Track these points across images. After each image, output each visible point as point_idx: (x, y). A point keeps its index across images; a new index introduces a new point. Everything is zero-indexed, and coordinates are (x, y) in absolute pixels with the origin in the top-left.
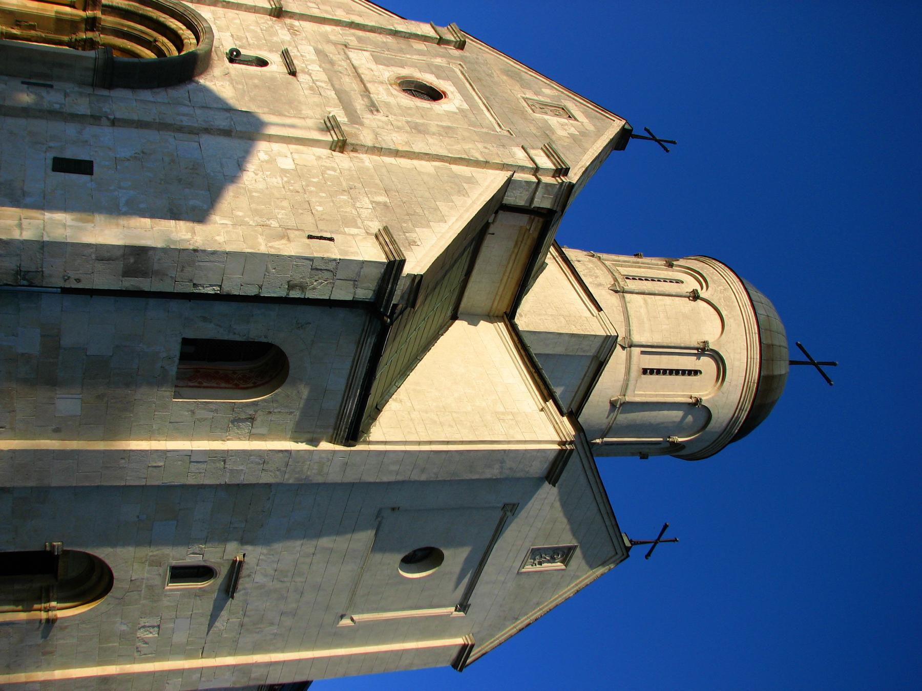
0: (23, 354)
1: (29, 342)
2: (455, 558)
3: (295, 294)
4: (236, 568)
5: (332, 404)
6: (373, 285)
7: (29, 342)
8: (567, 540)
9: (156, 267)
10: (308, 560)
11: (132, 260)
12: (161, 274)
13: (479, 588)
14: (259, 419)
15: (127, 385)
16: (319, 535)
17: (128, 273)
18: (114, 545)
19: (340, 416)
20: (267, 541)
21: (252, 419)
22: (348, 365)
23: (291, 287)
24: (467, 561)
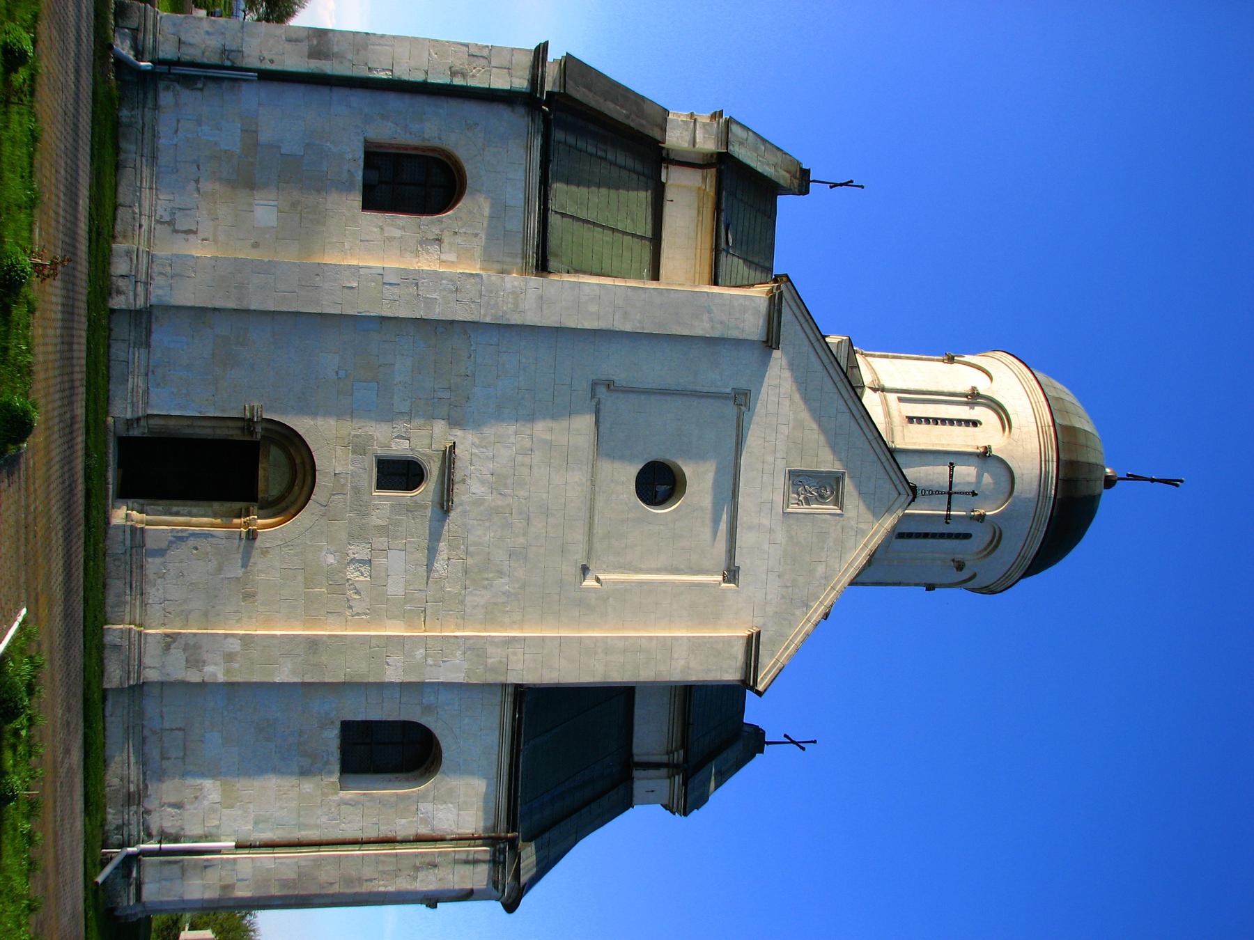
0: (226, 152)
2: (700, 479)
3: (458, 81)
5: (515, 224)
6: (527, 74)
7: (230, 138)
8: (827, 462)
9: (336, 49)
10: (527, 460)
11: (315, 42)
12: (340, 56)
14: (446, 240)
15: (319, 191)
16: (532, 418)
18: (314, 414)
20: (477, 425)
21: (439, 240)
22: (520, 174)
23: (453, 74)
24: (717, 484)
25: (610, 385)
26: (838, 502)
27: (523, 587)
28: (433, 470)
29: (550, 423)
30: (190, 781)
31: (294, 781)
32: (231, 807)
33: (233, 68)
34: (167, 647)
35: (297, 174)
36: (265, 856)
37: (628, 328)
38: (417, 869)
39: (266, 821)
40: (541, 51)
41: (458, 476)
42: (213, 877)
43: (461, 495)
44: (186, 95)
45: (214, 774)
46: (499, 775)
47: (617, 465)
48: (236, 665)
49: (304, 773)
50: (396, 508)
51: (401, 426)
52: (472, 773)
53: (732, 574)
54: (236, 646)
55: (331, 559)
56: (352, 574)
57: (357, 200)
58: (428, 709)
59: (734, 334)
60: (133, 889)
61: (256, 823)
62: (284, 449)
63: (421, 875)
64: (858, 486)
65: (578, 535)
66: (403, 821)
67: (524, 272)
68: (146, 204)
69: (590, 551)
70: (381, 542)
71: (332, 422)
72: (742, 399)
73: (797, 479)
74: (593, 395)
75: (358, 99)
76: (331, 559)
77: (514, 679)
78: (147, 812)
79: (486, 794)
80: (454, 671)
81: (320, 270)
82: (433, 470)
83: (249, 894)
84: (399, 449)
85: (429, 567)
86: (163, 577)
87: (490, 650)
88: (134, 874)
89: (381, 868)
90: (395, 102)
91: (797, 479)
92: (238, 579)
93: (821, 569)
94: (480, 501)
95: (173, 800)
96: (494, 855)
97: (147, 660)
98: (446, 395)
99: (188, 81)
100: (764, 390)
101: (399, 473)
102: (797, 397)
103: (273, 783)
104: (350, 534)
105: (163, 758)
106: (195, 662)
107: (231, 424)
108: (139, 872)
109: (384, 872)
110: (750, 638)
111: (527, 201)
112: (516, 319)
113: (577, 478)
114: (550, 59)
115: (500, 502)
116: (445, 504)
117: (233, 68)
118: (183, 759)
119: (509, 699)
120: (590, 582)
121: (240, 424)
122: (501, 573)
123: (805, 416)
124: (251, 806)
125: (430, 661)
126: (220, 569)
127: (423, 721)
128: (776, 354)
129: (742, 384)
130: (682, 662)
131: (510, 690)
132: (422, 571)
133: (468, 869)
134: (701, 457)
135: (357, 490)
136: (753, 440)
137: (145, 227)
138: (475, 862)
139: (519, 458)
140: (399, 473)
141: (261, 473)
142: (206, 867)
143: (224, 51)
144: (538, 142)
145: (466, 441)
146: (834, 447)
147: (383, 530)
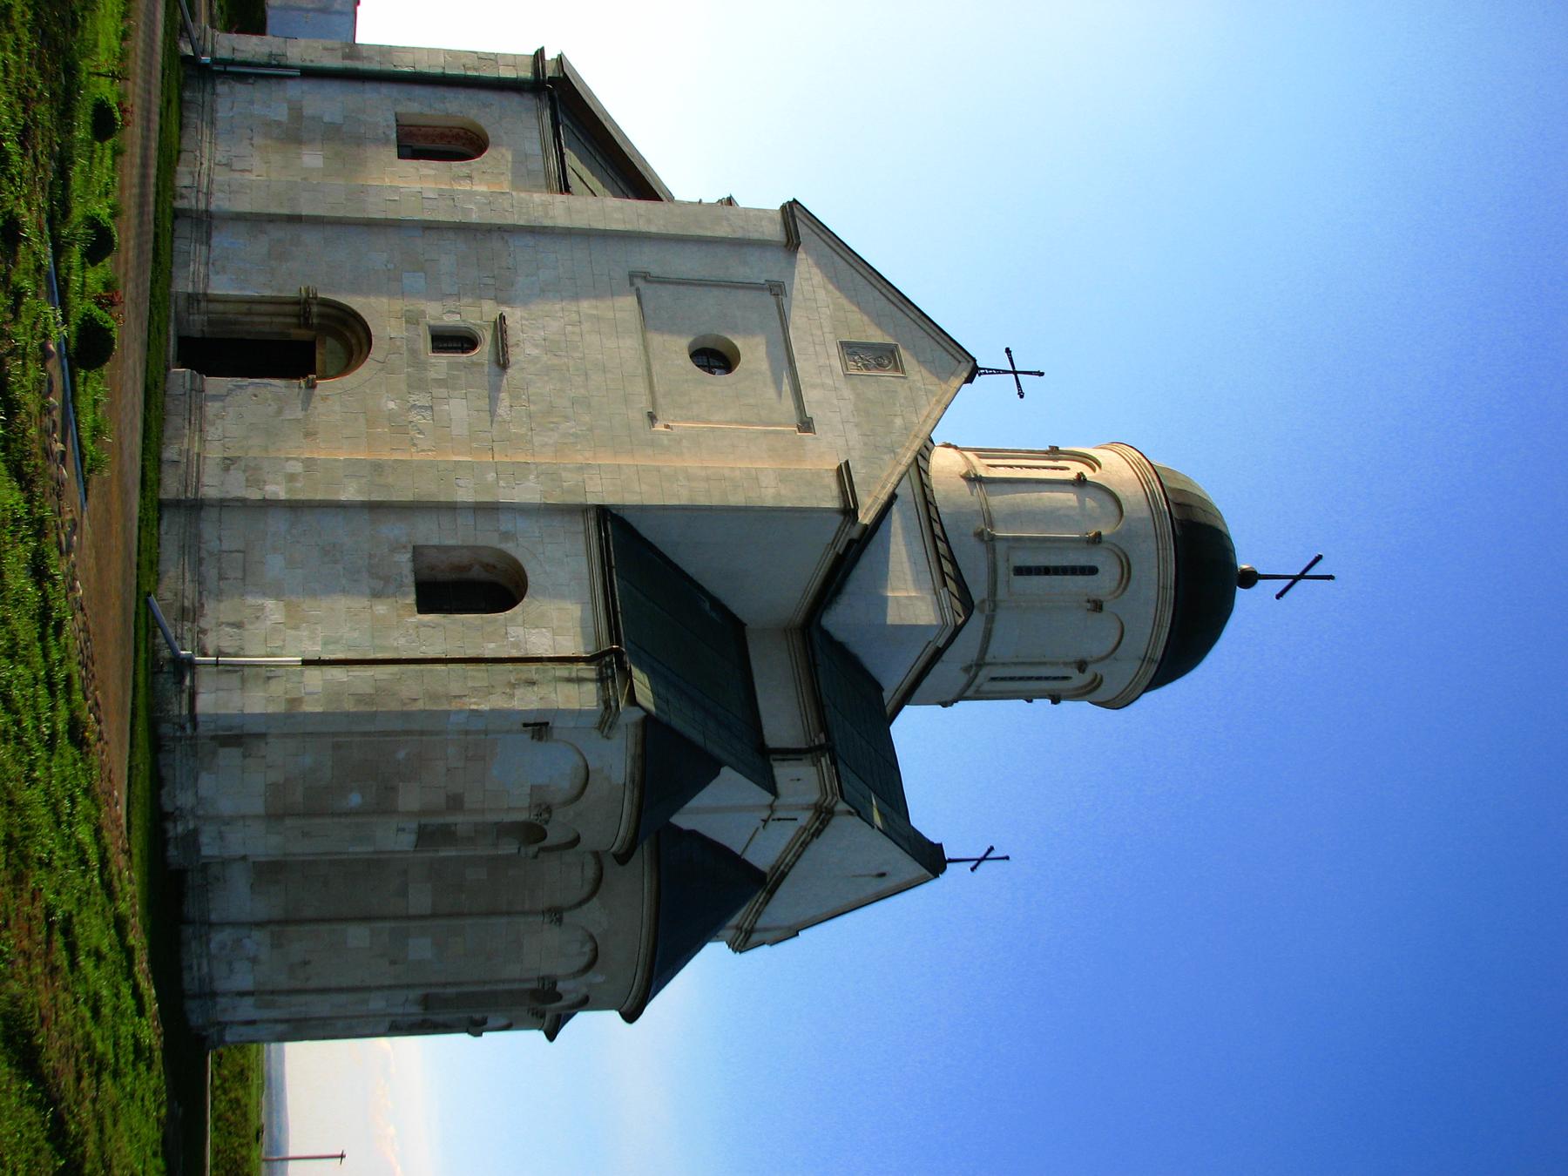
1: (281, 113)
2: (753, 352)
4: (500, 325)
5: (537, 164)
7: (281, 113)
8: (877, 336)
10: (577, 329)
13: (809, 396)
14: (474, 174)
15: (358, 145)
16: (576, 297)
17: (345, 57)
19: (547, 175)
20: (525, 304)
21: (470, 177)
22: (536, 134)
25: (646, 277)
26: (898, 366)
27: (591, 429)
28: (487, 337)
29: (594, 302)
30: (250, 600)
31: (365, 602)
32: (296, 628)
33: (278, 66)
34: (227, 469)
35: (344, 138)
36: (338, 673)
37: (653, 229)
38: (513, 686)
39: (336, 642)
40: (540, 54)
41: (511, 340)
42: (277, 688)
43: (514, 355)
44: (239, 88)
45: (277, 592)
46: (592, 590)
47: (666, 337)
48: (299, 485)
49: (376, 595)
50: (451, 366)
51: (451, 304)
52: (562, 597)
53: (806, 425)
54: (298, 468)
55: (392, 405)
56: (414, 417)
57: (394, 151)
58: (506, 536)
59: (755, 236)
60: (185, 696)
61: (325, 644)
62: (339, 336)
63: (519, 692)
64: (916, 355)
65: (640, 387)
66: (492, 645)
67: (550, 189)
68: (206, 151)
69: (654, 403)
70: (443, 392)
71: (385, 300)
72: (777, 290)
73: (850, 349)
74: (632, 284)
75: (386, 90)
76: (392, 405)
77: (593, 500)
78: (203, 632)
79: (582, 619)
80: (529, 492)
81: (364, 189)
82: (487, 337)
83: (319, 709)
84: (451, 320)
85: (492, 413)
86: (222, 418)
87: (564, 474)
88: (187, 682)
89: (470, 684)
90: (419, 91)
91: (850, 349)
92: (298, 420)
93: (898, 422)
95: (232, 619)
96: (601, 673)
97: (206, 480)
98: (491, 281)
99: (242, 78)
100: (797, 280)
101: (453, 341)
102: (830, 287)
103: (342, 603)
104: (409, 386)
105: (221, 578)
106: (257, 483)
107: (287, 309)
108: (193, 680)
109: (474, 689)
110: (839, 469)
111: (544, 150)
112: (548, 223)
113: (628, 346)
115: (556, 361)
116: (502, 363)
117: (278, 66)
118: (243, 579)
119: (592, 524)
120: (659, 427)
121: (297, 308)
122: (567, 418)
123: (844, 302)
124: (319, 627)
125: (502, 483)
126: (280, 412)
128: (801, 255)
130: (771, 491)
131: (592, 514)
132: (486, 415)
133: (572, 689)
134: (748, 332)
135: (413, 352)
136: (797, 318)
137: (205, 165)
139: (569, 328)
140: (453, 341)
142: (269, 678)
143: (270, 55)
144: (547, 113)
145: (515, 317)
146: (879, 325)
147: (441, 383)
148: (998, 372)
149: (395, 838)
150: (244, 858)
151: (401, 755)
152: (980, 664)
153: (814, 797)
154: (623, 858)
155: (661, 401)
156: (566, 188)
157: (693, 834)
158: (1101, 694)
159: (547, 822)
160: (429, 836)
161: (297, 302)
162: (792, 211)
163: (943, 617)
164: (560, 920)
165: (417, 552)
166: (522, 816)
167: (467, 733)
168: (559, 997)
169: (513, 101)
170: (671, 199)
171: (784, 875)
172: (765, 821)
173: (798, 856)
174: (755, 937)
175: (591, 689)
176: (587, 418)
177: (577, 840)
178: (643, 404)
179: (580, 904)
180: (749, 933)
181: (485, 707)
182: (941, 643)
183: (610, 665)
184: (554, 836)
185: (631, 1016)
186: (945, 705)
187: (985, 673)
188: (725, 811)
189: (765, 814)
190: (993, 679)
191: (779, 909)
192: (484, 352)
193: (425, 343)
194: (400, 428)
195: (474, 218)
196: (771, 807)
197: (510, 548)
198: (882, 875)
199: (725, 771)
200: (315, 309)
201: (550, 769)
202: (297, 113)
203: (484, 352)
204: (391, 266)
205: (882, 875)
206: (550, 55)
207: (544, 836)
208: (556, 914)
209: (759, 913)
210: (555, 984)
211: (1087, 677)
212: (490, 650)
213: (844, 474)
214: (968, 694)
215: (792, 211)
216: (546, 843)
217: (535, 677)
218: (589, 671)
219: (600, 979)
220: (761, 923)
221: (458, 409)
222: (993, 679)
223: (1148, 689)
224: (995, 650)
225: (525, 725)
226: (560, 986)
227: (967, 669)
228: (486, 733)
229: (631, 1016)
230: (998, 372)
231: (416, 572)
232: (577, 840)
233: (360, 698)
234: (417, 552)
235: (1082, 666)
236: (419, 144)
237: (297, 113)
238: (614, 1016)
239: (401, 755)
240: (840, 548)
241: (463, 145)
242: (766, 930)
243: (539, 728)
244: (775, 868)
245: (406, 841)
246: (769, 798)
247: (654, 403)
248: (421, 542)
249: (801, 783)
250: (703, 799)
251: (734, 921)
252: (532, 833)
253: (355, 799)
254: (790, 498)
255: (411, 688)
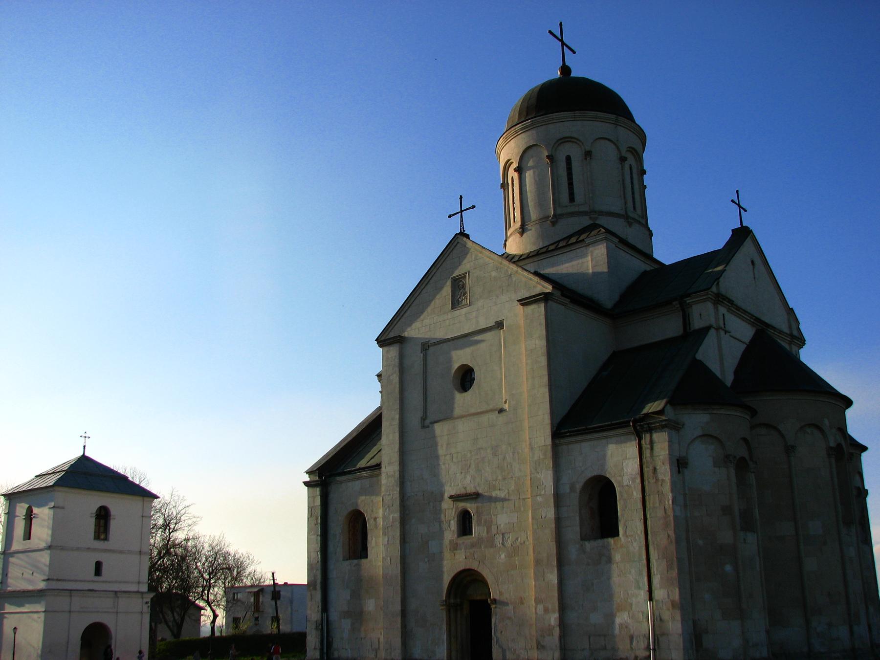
1: (346, 624)
2: (460, 357)
4: (455, 498)
7: (346, 624)
8: (447, 290)
10: (455, 456)
13: (483, 325)
14: (373, 516)
16: (437, 457)
17: (315, 589)
18: (442, 572)
19: (371, 476)
20: (442, 486)
21: (375, 519)
22: (350, 484)
24: (462, 347)
25: (424, 419)
26: (463, 276)
27: (510, 444)
29: (439, 447)
30: (617, 631)
31: (614, 567)
32: (631, 605)
33: (322, 625)
34: (543, 647)
36: (656, 580)
37: (397, 416)
38: (657, 480)
39: (638, 582)
40: (306, 483)
41: (463, 491)
42: (666, 615)
43: (471, 489)
44: (335, 645)
45: (610, 617)
46: (599, 439)
47: (456, 406)
48: (550, 607)
49: (610, 560)
50: (479, 523)
51: (445, 526)
52: (605, 456)
53: (499, 325)
54: (540, 608)
55: (503, 556)
56: (508, 544)
57: (364, 561)
58: (572, 489)
59: (397, 361)
61: (639, 588)
63: (661, 477)
64: (456, 267)
65: (484, 419)
66: (635, 493)
67: (379, 475)
69: (492, 410)
71: (445, 563)
72: (426, 346)
73: (456, 304)
74: (428, 427)
75: (331, 565)
76: (503, 556)
77: (549, 441)
78: (636, 658)
79: (616, 443)
80: (547, 477)
81: (385, 576)
82: (462, 505)
83: (677, 590)
84: (454, 525)
85: (504, 500)
86: (515, 650)
87: (536, 458)
89: (658, 505)
90: (331, 548)
91: (456, 304)
93: (494, 274)
94: (473, 478)
95: (628, 642)
96: (647, 431)
98: (431, 504)
99: (330, 644)
100: (419, 336)
101: (465, 524)
102: (422, 317)
103: (615, 579)
104: (491, 547)
106: (550, 629)
109: (660, 502)
110: (523, 305)
111: (358, 479)
112: (397, 475)
113: (462, 426)
114: (308, 479)
115: (473, 466)
116: (475, 496)
117: (322, 625)
118: (605, 636)
119: (562, 441)
120: (506, 407)
122: (504, 458)
123: (429, 309)
124: (630, 592)
125: (543, 492)
126: (509, 618)
127: (578, 491)
128: (406, 334)
129: (419, 348)
130: (537, 342)
131: (557, 441)
132: (506, 504)
133: (657, 447)
134: (450, 361)
135: (473, 545)
136: (440, 334)
138: (652, 443)
139: (455, 460)
140: (465, 524)
141: (478, 598)
142: (661, 620)
144: (338, 478)
145: (449, 491)
146: (442, 288)
148: (462, 221)
149: (750, 544)
150: (767, 632)
151: (701, 542)
152: (626, 217)
153: (710, 305)
154: (753, 413)
155: (491, 407)
156: (378, 466)
157: (736, 373)
158: (638, 147)
159: (735, 457)
160: (747, 525)
161: (449, 612)
162: (383, 341)
163: (601, 240)
164: (793, 447)
165: (584, 538)
166: (732, 471)
167: (685, 506)
168: (839, 445)
169: (333, 496)
170: (380, 408)
171: (758, 320)
172: (726, 332)
173: (745, 312)
174: (795, 333)
175: (655, 436)
176: (504, 447)
177: (745, 440)
178: (494, 416)
179: (782, 436)
180: (792, 335)
181: (670, 496)
182: (616, 240)
183: (642, 426)
184: (742, 452)
185: (848, 403)
186: (651, 234)
187: (631, 214)
188: (722, 355)
189: (722, 333)
190: (634, 208)
191: (779, 322)
192: (470, 507)
193: (467, 539)
194: (515, 551)
195: (397, 515)
196: (717, 329)
197: (579, 487)
198: (753, 262)
199: (699, 356)
200: (452, 601)
201: (703, 457)
202: (347, 614)
203: (470, 507)
204: (426, 560)
205: (753, 262)
206: (307, 478)
207: (743, 459)
208: (789, 450)
209: (781, 332)
210: (831, 448)
211: (629, 156)
212: (637, 495)
213: (525, 302)
214: (644, 222)
215: (383, 341)
216: (747, 458)
217: (651, 468)
218: (646, 438)
219: (826, 422)
220: (786, 330)
221: (503, 519)
222: (634, 208)
223: (633, 120)
224: (617, 208)
225: (679, 472)
226: (832, 444)
227: (630, 225)
228: (685, 495)
229: (848, 403)
230: (462, 221)
231: (595, 539)
232: (745, 440)
233: (669, 567)
234: (584, 538)
235: (623, 159)
236: (359, 547)
237: (347, 614)
238: (848, 412)
239: (701, 542)
240: (567, 301)
241: (358, 525)
242: (790, 327)
243: (680, 464)
244: (752, 324)
245: (751, 538)
246: (712, 332)
247: (492, 410)
248: (579, 537)
249: (703, 313)
250: (715, 367)
251: (787, 346)
252: (742, 466)
253: (728, 568)
254: (540, 331)
255: (662, 538)
